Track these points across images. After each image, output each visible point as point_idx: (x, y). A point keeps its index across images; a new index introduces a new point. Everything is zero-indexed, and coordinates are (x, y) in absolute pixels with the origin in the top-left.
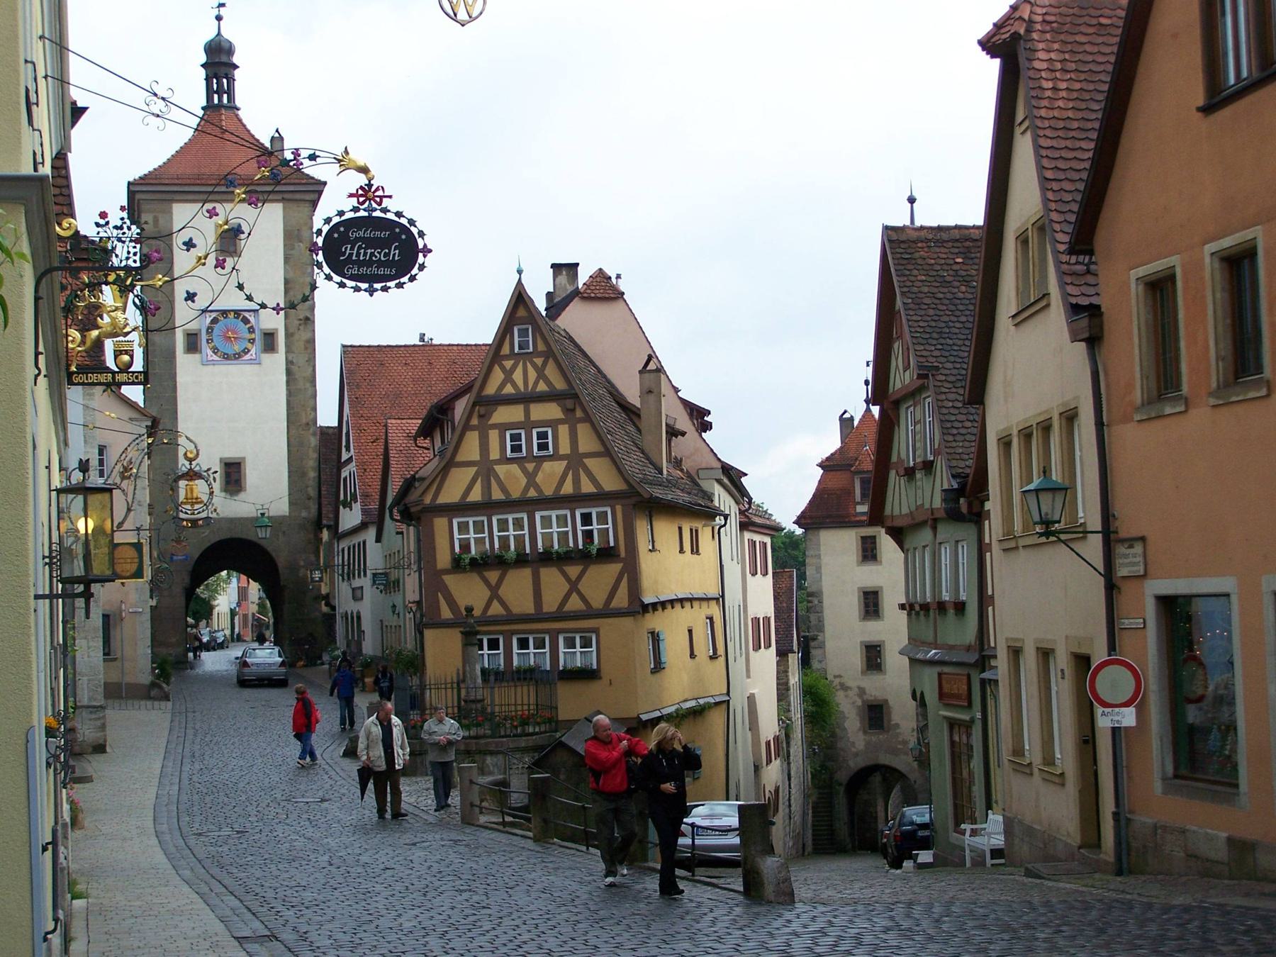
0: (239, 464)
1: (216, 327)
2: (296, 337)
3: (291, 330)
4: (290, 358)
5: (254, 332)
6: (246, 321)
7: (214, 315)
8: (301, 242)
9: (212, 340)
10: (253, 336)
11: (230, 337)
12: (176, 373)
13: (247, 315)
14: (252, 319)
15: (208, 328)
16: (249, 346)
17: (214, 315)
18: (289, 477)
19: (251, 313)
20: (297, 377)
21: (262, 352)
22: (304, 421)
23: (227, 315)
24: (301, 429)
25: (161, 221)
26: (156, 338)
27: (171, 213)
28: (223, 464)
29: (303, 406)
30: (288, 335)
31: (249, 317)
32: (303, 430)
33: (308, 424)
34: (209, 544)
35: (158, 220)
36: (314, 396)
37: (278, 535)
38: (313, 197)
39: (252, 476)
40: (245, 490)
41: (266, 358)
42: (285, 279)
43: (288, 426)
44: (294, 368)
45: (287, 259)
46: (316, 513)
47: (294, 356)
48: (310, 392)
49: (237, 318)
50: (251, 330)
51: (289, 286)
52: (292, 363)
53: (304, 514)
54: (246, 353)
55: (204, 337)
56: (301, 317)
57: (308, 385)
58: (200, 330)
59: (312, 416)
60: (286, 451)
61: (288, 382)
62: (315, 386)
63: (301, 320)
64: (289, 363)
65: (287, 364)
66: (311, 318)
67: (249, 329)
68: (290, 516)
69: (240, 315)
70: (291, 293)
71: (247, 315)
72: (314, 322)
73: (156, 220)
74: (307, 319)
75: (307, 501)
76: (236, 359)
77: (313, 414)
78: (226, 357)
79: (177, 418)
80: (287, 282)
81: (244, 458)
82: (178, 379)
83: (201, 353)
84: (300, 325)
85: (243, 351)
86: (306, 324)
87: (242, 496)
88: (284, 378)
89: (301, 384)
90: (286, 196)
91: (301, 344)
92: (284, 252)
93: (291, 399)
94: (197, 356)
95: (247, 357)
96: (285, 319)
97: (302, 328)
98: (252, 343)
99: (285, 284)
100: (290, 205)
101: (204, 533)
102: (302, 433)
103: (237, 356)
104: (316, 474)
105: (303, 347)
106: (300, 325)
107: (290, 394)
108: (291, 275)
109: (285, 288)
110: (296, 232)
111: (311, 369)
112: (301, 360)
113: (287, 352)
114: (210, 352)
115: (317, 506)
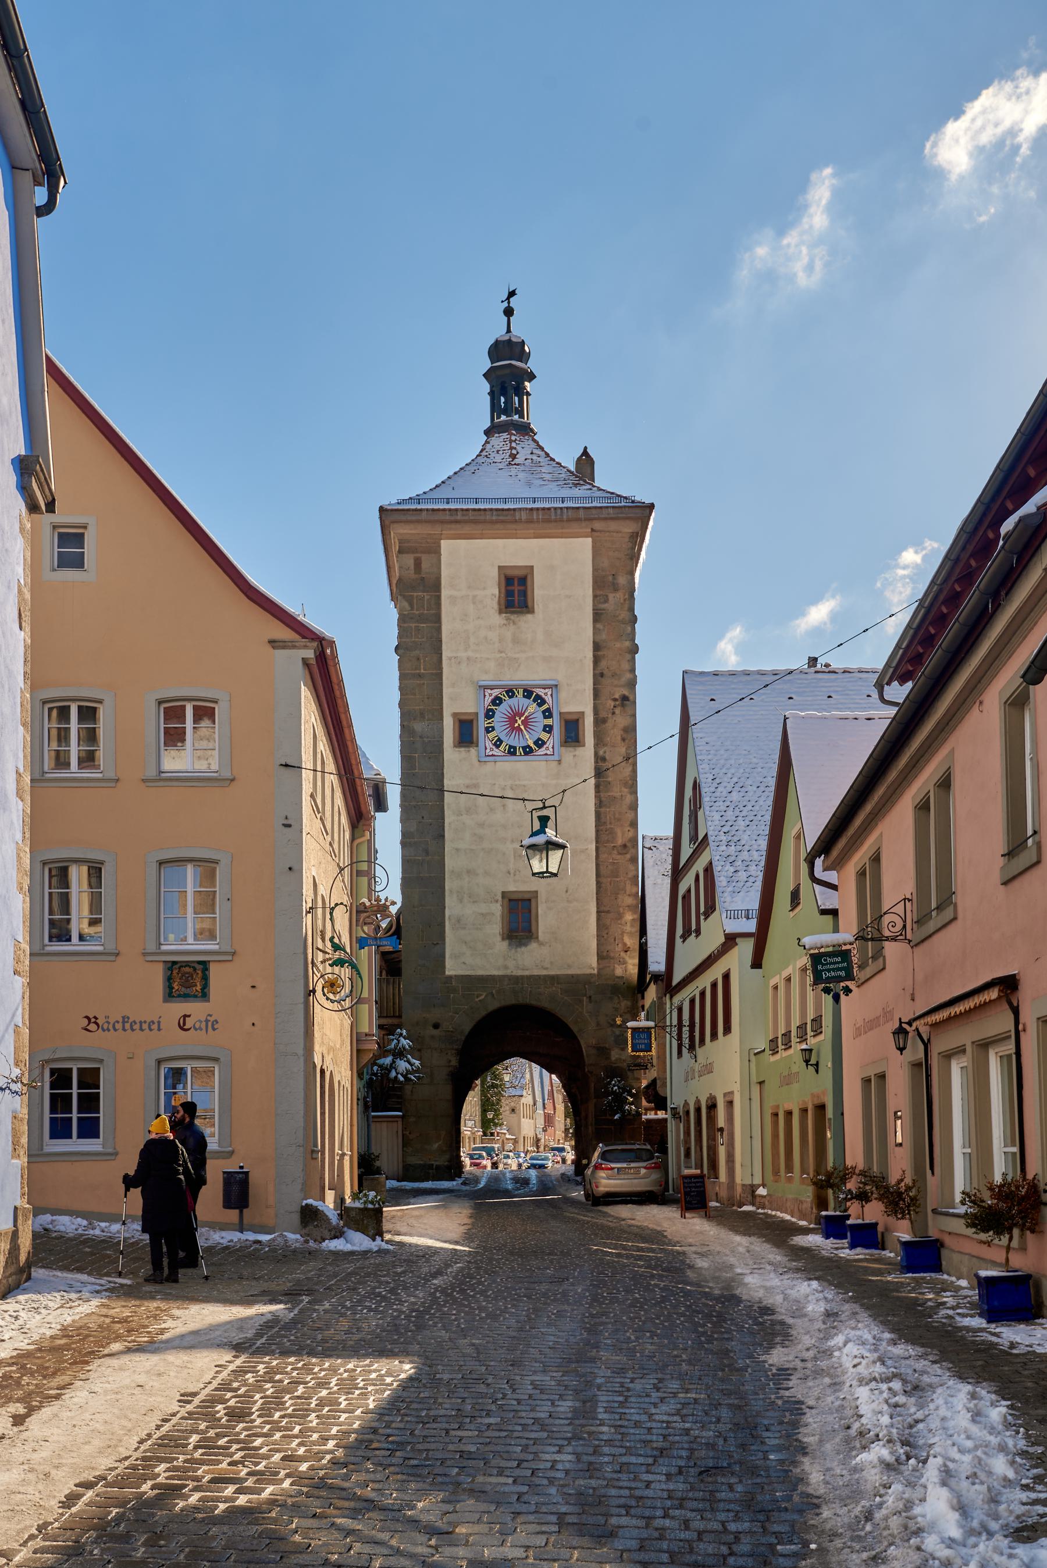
1: (502, 711)
2: (609, 724)
3: (603, 714)
4: (601, 753)
5: (550, 716)
6: (540, 701)
7: (496, 692)
9: (493, 729)
10: (549, 722)
14: (548, 699)
15: (488, 710)
16: (544, 736)
20: (610, 779)
22: (620, 842)
23: (514, 693)
24: (615, 852)
28: (506, 900)
30: (599, 721)
32: (620, 854)
33: (625, 846)
34: (484, 1013)
36: (634, 807)
37: (581, 1001)
39: (546, 920)
41: (568, 755)
42: (594, 642)
45: (598, 616)
46: (636, 971)
48: (629, 799)
50: (548, 714)
51: (599, 653)
52: (604, 759)
54: (540, 746)
55: (482, 723)
56: (617, 696)
58: (477, 714)
59: (631, 834)
63: (615, 700)
64: (599, 759)
65: (596, 762)
66: (631, 698)
67: (544, 712)
70: (603, 664)
71: (541, 692)
72: (635, 702)
74: (625, 698)
75: (623, 954)
76: (526, 754)
77: (632, 830)
78: (512, 751)
79: (443, 836)
80: (597, 647)
81: (536, 892)
83: (477, 746)
84: (615, 707)
86: (623, 705)
87: (533, 945)
89: (617, 791)
90: (597, 525)
92: (594, 605)
93: (602, 810)
94: (473, 751)
95: (542, 751)
97: (617, 711)
98: (549, 732)
99: (594, 650)
101: (477, 997)
103: (528, 751)
104: (637, 916)
105: (619, 738)
107: (600, 804)
108: (604, 636)
109: (594, 656)
110: (610, 578)
111: (630, 769)
112: (615, 754)
114: (489, 745)
115: (636, 961)
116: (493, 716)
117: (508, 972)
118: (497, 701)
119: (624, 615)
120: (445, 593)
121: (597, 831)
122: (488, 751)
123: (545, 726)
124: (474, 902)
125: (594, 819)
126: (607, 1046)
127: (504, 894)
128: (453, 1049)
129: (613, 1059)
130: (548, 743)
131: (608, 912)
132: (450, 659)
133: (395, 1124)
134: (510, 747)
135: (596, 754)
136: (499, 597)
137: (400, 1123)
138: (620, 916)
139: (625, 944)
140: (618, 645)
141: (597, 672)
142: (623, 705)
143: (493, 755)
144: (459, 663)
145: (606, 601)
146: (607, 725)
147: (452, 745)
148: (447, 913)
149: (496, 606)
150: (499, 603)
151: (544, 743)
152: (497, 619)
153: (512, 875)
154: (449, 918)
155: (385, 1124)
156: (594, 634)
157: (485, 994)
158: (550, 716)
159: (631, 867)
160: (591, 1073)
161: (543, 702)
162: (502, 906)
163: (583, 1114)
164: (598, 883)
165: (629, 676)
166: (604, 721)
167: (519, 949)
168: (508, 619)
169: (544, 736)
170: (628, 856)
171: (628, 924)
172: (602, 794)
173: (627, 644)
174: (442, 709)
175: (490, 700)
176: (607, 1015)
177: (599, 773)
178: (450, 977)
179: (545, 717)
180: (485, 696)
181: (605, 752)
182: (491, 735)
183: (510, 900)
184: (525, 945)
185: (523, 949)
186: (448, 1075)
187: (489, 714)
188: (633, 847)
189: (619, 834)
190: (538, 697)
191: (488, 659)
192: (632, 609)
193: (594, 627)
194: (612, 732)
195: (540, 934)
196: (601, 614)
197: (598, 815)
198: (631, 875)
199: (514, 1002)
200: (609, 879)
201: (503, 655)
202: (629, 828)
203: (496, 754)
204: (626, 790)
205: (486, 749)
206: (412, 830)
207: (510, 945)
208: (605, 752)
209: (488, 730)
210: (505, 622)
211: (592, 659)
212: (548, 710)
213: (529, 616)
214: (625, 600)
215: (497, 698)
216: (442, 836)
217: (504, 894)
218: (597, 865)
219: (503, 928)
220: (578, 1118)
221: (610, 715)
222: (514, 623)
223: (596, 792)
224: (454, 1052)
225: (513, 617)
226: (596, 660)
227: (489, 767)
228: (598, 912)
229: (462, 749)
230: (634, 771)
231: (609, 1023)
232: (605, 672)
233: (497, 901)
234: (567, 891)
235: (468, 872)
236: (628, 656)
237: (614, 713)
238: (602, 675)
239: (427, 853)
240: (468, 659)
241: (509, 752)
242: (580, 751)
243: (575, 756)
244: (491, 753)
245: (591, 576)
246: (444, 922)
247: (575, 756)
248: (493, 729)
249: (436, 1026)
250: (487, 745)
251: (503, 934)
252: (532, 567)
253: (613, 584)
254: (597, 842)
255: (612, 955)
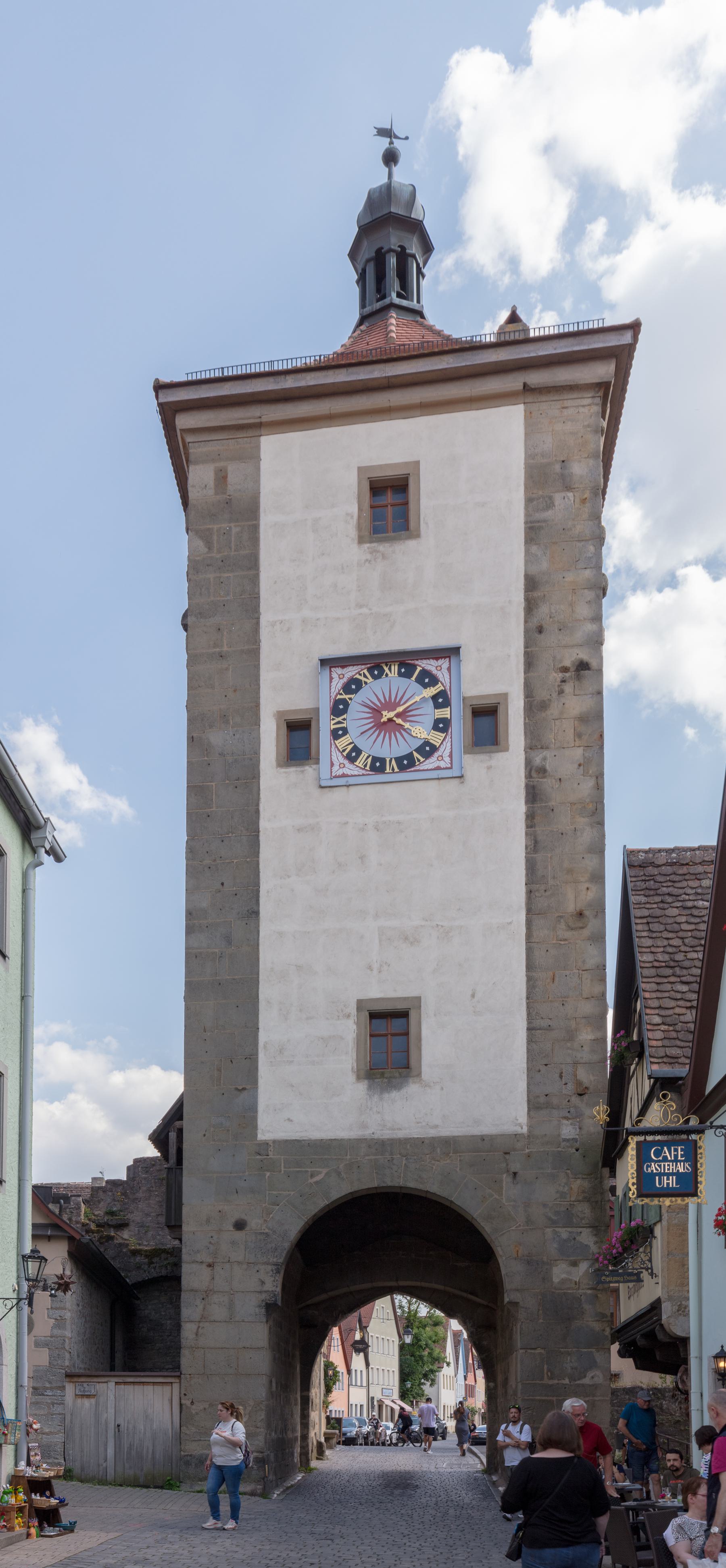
0: (404, 1015)
2: (554, 711)
3: (541, 694)
4: (537, 761)
5: (447, 703)
8: (568, 488)
10: (445, 713)
11: (390, 720)
12: (257, 812)
13: (430, 665)
14: (443, 676)
15: (337, 702)
16: (436, 738)
17: (351, 672)
18: (530, 1041)
19: (444, 663)
21: (465, 753)
24: (563, 925)
25: (236, 474)
26: (217, 738)
27: (255, 457)
29: (570, 871)
31: (434, 671)
33: (581, 914)
35: (225, 478)
38: (604, 371)
40: (419, 1075)
43: (529, 924)
44: (547, 784)
47: (546, 753)
48: (587, 836)
49: (408, 675)
50: (441, 700)
51: (536, 594)
52: (542, 771)
53: (568, 1131)
55: (326, 724)
56: (567, 663)
57: (582, 821)
58: (317, 710)
59: (591, 895)
60: (524, 979)
61: (530, 818)
62: (601, 823)
63: (565, 670)
65: (529, 776)
66: (594, 663)
68: (530, 1137)
69: (414, 667)
70: (544, 610)
73: (221, 478)
74: (582, 666)
75: (575, 1100)
76: (402, 768)
77: (594, 888)
78: (378, 766)
79: (257, 913)
80: (531, 584)
81: (418, 999)
82: (263, 824)
83: (317, 761)
84: (563, 681)
85: (419, 750)
86: (578, 678)
87: (412, 1088)
88: (520, 808)
91: (568, 728)
92: (527, 515)
93: (539, 857)
94: (309, 770)
95: (431, 763)
96: (526, 671)
97: (568, 688)
98: (444, 730)
100: (549, 407)
101: (312, 1176)
102: (568, 934)
103: (406, 763)
105: (570, 733)
106: (563, 681)
107: (534, 846)
108: (545, 565)
110: (557, 467)
111: (591, 783)
113: (530, 747)
114: (337, 758)
116: (345, 711)
117: (367, 1133)
118: (353, 686)
119: (582, 527)
120: (267, 519)
121: (529, 892)
122: (336, 768)
123: (437, 721)
124: (308, 1018)
125: (523, 872)
126: (545, 1259)
127: (360, 1004)
128: (268, 1263)
129: (556, 1280)
130: (442, 749)
131: (549, 1028)
132: (273, 624)
133: (167, 1388)
134: (375, 759)
135: (528, 763)
136: (359, 517)
137: (176, 1387)
138: (571, 1035)
139: (579, 1083)
140: (570, 577)
141: (535, 622)
142: (578, 678)
143: (344, 776)
144: (288, 629)
145: (550, 504)
146: (548, 712)
147: (274, 763)
148: (263, 1037)
149: (353, 533)
150: (359, 528)
151: (434, 749)
152: (355, 553)
153: (375, 972)
154: (265, 1047)
155: (150, 1388)
156: (527, 562)
157: (324, 1171)
158: (447, 703)
159: (592, 950)
160: (516, 1304)
161: (434, 681)
162: (358, 1024)
163: (500, 1378)
164: (529, 979)
165: (590, 627)
166: (544, 706)
167: (386, 1095)
168: (373, 552)
169: (436, 738)
170: (586, 932)
171: (586, 1048)
172: (538, 830)
173: (588, 573)
174: (257, 705)
175: (340, 685)
176: (545, 1205)
177: (533, 795)
178: (266, 1144)
179: (437, 706)
180: (331, 679)
181: (545, 759)
182: (342, 742)
183: (374, 1016)
184: (398, 1087)
185: (394, 1094)
186: (259, 1306)
187: (339, 708)
188: (596, 916)
189: (571, 895)
190: (425, 673)
191: (338, 619)
192: (596, 517)
193: (527, 552)
194: (557, 722)
195: (424, 1068)
196: (540, 528)
197: (531, 867)
198: (591, 963)
199: (375, 1184)
200: (551, 974)
201: (365, 610)
202: (587, 885)
203: (349, 772)
204: (586, 820)
205: (332, 765)
206: (204, 905)
207: (370, 1088)
208: (545, 759)
209: (336, 734)
210: (369, 557)
211: (523, 605)
212: (442, 694)
213: (412, 544)
214: (584, 501)
215: (353, 680)
216: (255, 914)
217: (360, 1004)
218: (529, 951)
219: (358, 1060)
220: (492, 1385)
221: (555, 695)
222: (384, 557)
223: (528, 827)
224: (270, 1267)
225: (383, 547)
226: (530, 606)
227: (338, 795)
228: (529, 1029)
229: (292, 769)
230: (599, 787)
231: (550, 1219)
232: (545, 626)
233: (348, 1016)
234: (473, 996)
235: (299, 968)
236: (589, 595)
237: (561, 692)
238: (540, 630)
239: (228, 940)
240: (304, 621)
241: (373, 768)
242: (499, 759)
243: (489, 768)
244: (340, 772)
245: (523, 466)
246: (257, 1054)
247: (489, 768)
248: (345, 731)
249: (240, 1225)
250: (334, 758)
251: (358, 1070)
252: (417, 463)
253: (563, 477)
254: (529, 911)
255: (555, 1101)
